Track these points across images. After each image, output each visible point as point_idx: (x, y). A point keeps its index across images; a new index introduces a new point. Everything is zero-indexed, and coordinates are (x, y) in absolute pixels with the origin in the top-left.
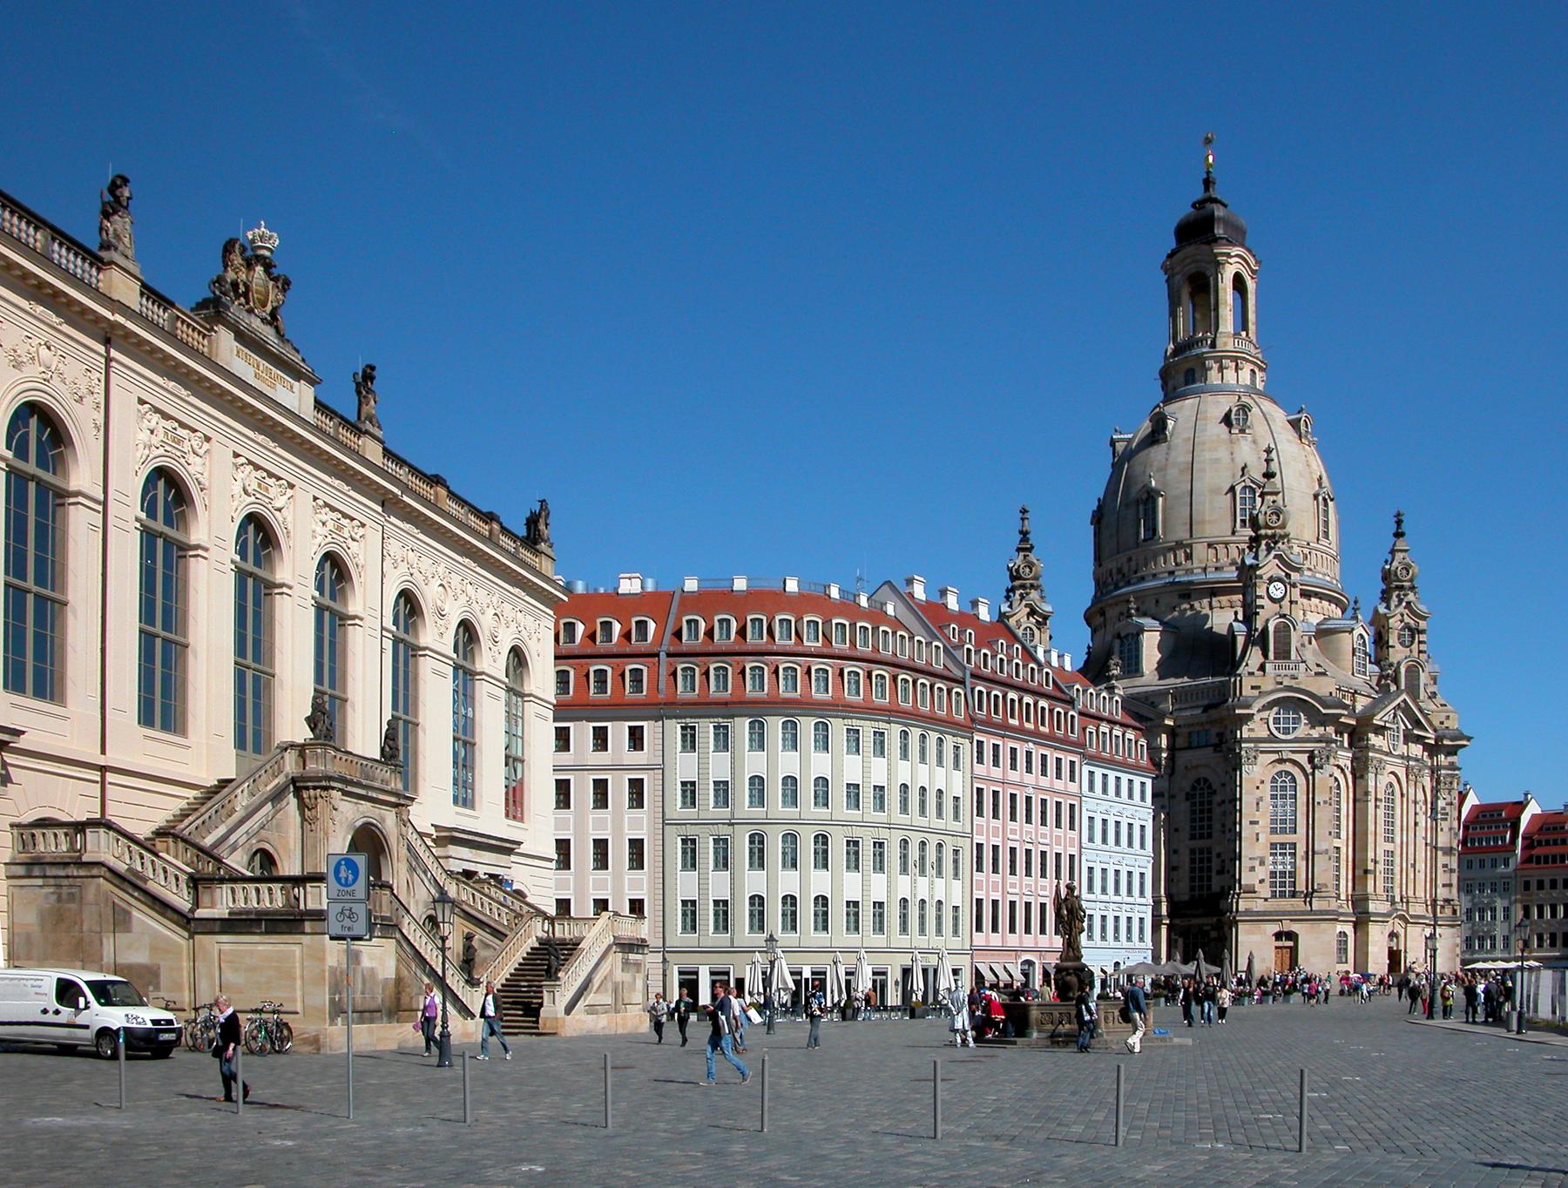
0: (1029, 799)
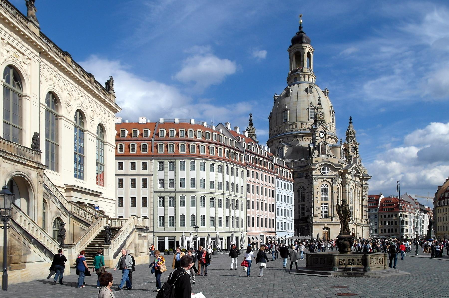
0: (262, 188)
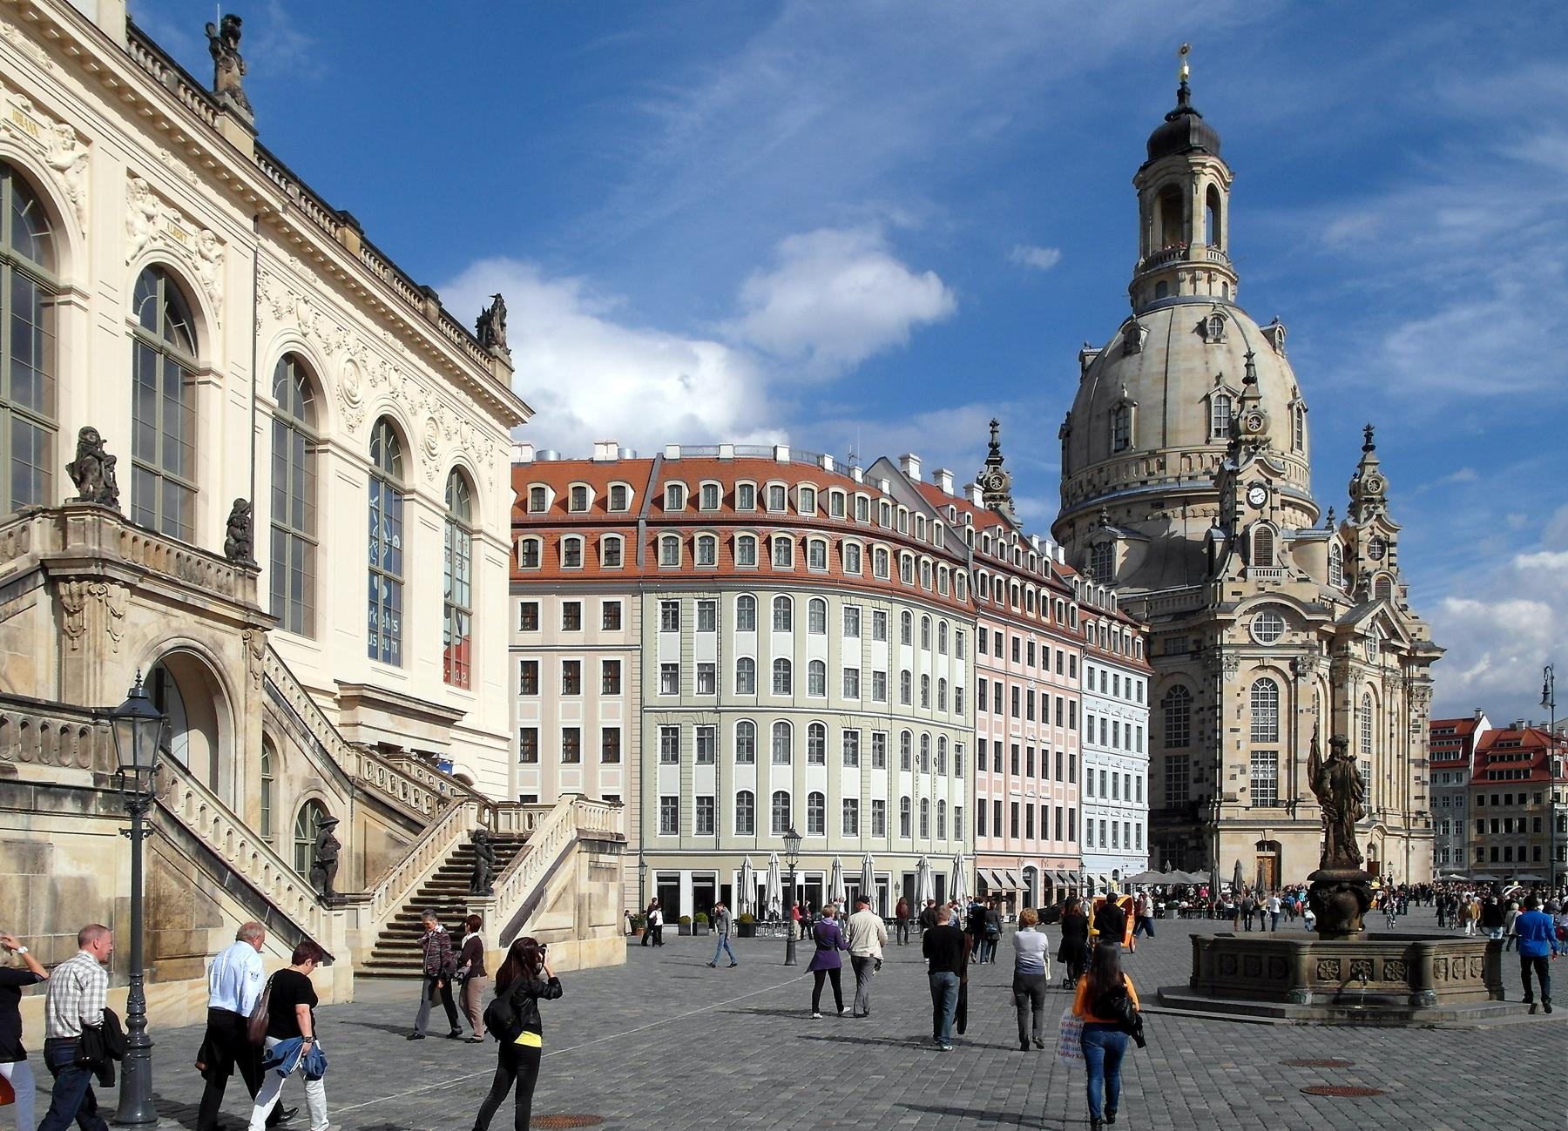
0: (1031, 693)
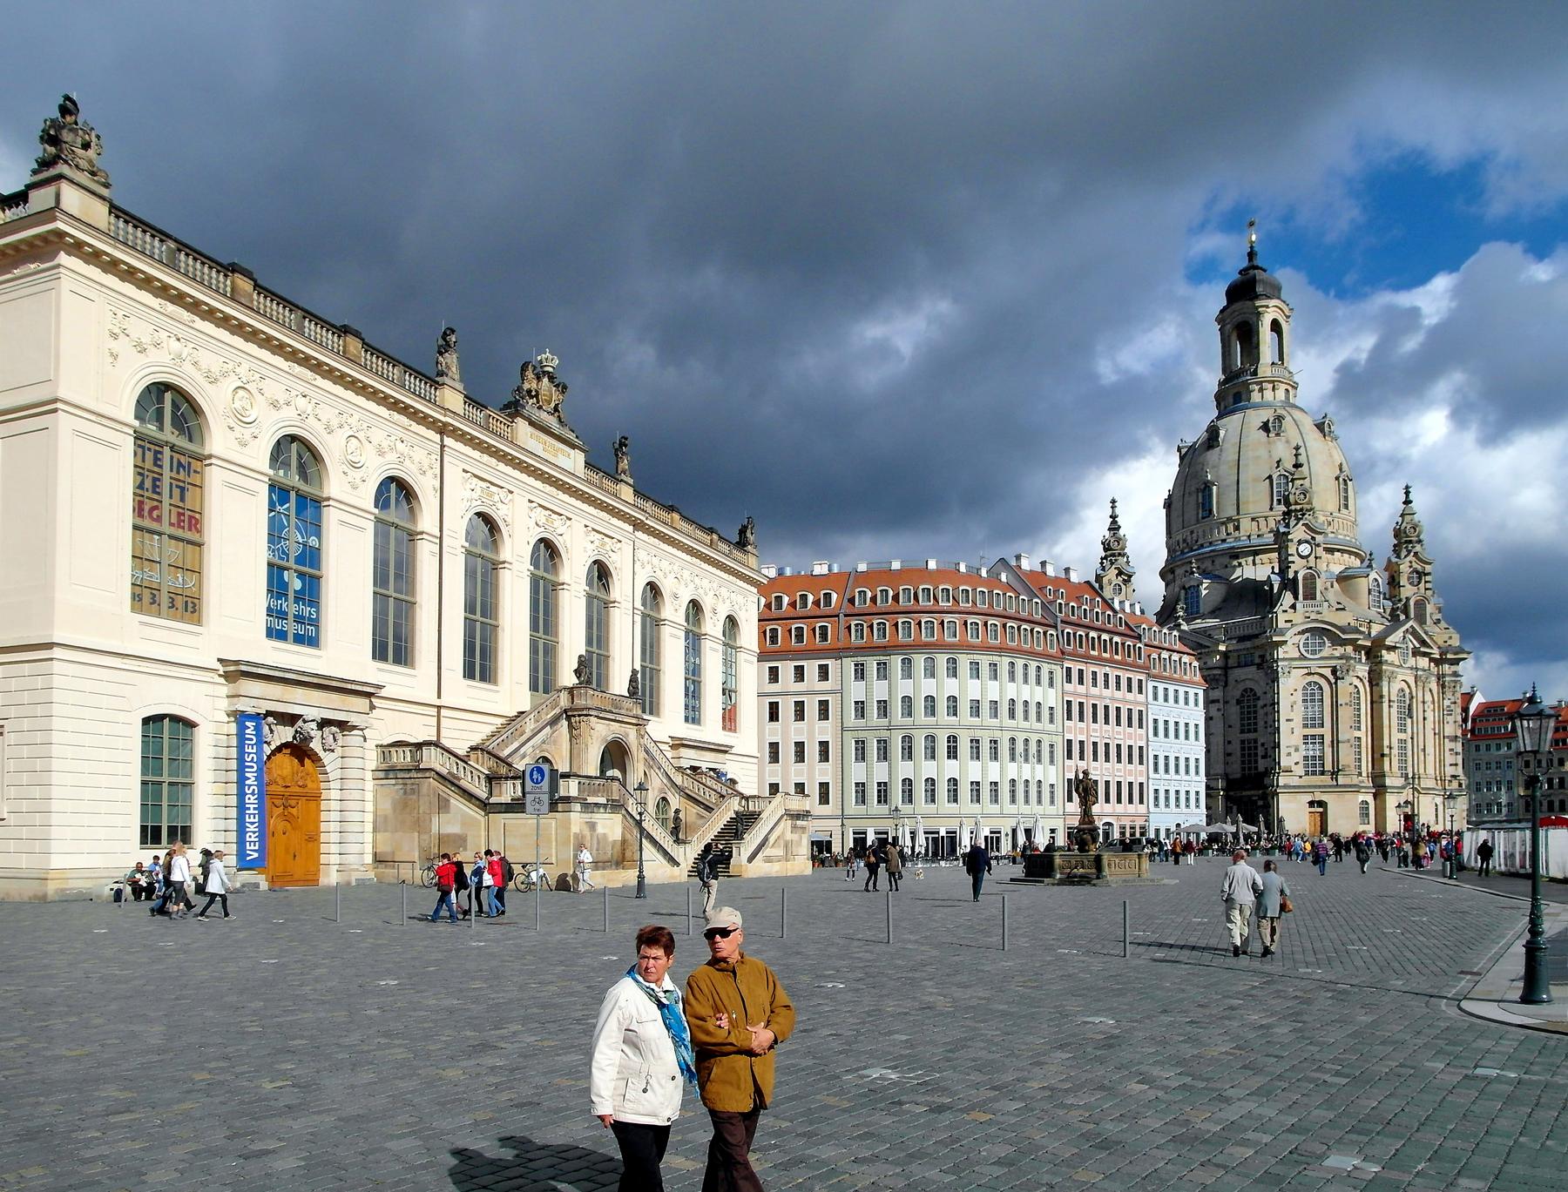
0: (1106, 708)
